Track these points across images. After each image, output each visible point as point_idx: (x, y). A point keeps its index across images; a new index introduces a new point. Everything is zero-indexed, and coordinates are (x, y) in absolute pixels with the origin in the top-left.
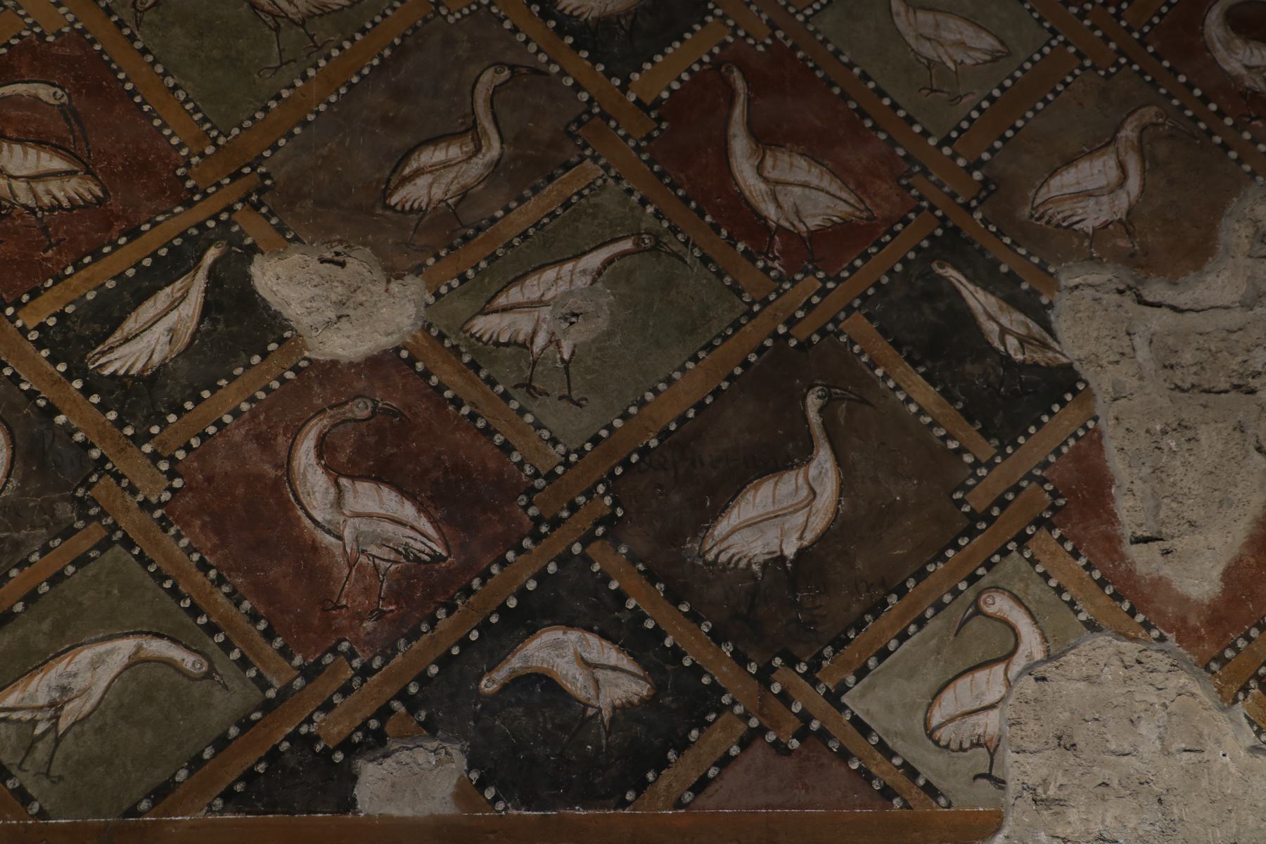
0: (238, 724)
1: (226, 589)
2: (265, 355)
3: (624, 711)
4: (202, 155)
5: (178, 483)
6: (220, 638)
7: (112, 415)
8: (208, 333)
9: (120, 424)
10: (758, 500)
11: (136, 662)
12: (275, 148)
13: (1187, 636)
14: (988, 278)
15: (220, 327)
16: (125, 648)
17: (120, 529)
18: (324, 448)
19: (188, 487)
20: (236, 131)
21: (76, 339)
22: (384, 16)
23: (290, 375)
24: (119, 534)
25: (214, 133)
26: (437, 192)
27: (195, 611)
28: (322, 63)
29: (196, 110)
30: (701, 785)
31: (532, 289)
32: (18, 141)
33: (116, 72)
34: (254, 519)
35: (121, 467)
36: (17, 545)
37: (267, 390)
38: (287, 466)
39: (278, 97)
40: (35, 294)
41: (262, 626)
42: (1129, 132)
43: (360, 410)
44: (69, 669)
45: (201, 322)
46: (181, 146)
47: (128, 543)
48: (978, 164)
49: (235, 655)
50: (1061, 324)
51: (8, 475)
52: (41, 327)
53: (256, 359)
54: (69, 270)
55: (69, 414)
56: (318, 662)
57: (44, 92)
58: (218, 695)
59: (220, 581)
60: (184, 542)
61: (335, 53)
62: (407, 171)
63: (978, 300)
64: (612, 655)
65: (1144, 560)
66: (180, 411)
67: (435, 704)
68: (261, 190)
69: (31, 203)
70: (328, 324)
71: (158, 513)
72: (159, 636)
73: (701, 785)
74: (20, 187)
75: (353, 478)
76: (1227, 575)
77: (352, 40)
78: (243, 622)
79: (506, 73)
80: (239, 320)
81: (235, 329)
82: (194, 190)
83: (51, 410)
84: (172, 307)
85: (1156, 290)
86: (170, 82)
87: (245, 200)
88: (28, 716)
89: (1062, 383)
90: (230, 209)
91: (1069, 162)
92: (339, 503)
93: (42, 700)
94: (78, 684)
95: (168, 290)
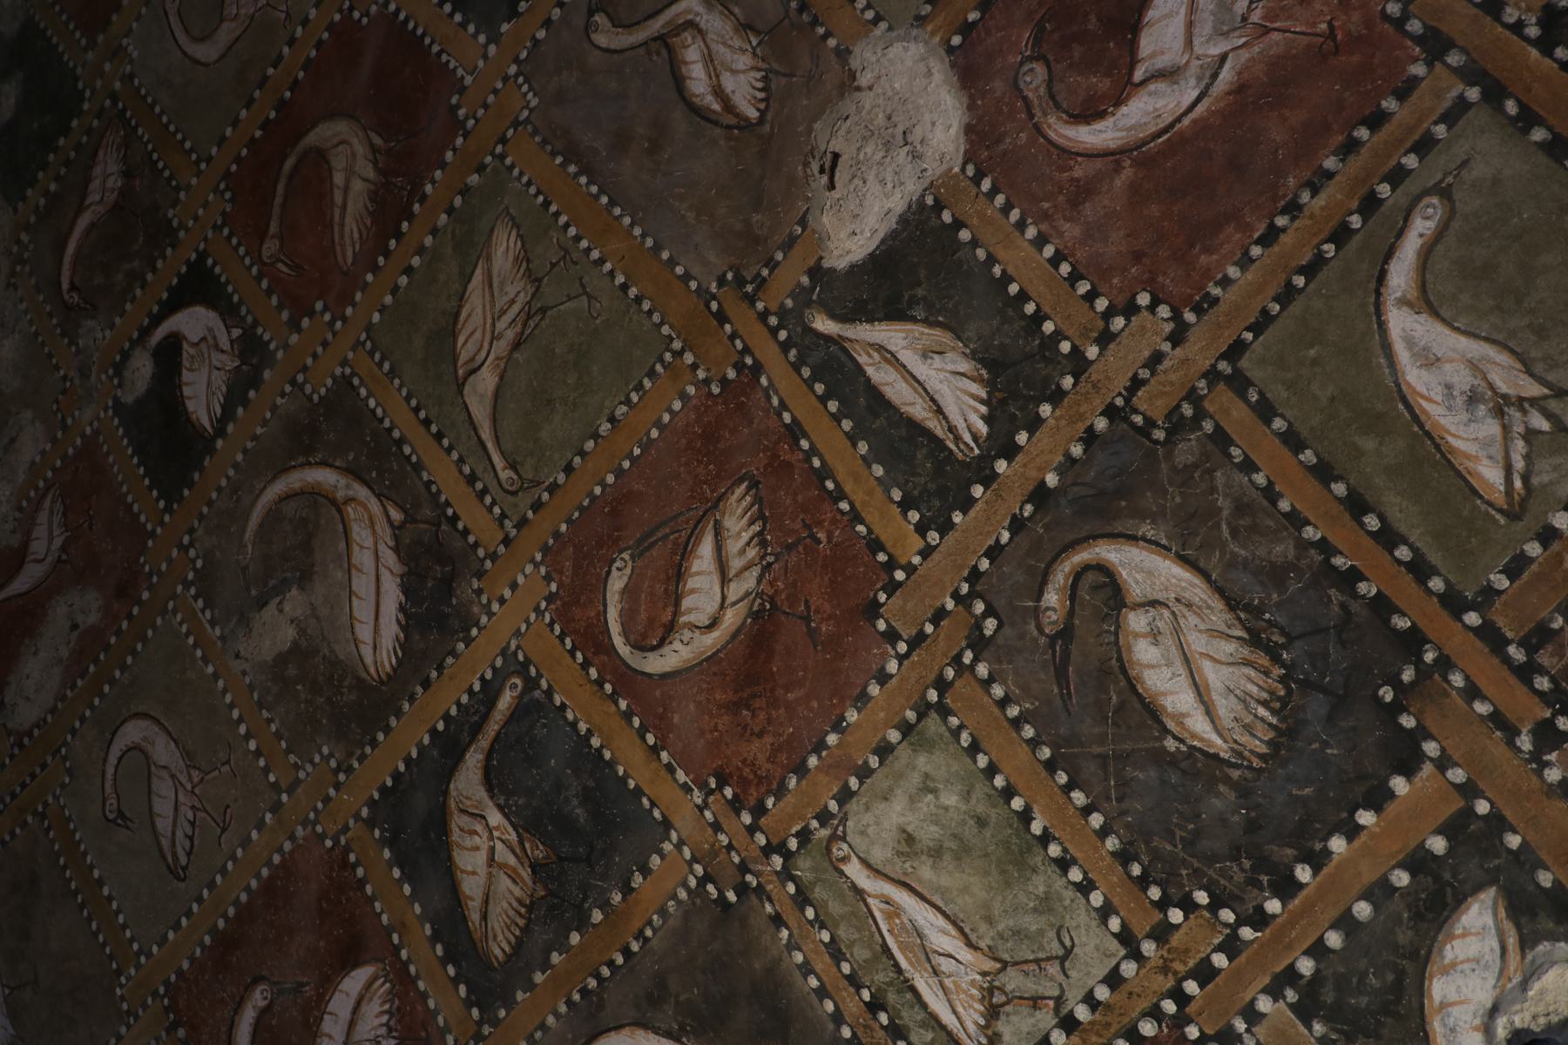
0: (1526, 130)
1: (1305, 197)
2: (958, 224)
4: (694, 367)
5: (1144, 299)
6: (1384, 190)
7: (1045, 410)
8: (930, 307)
9: (1057, 396)
11: (1426, 301)
12: (687, 277)
15: (920, 292)
16: (1399, 322)
17: (1214, 366)
18: (1089, 113)
19: (1150, 284)
20: (666, 330)
21: (935, 475)
22: (529, 183)
23: (986, 185)
24: (1224, 366)
25: (668, 356)
26: (744, 61)
27: (1341, 235)
28: (584, 244)
29: (639, 387)
32: (677, 604)
33: (594, 498)
34: (1196, 186)
35: (1122, 382)
36: (1241, 508)
37: (1006, 209)
38: (1113, 156)
39: (624, 287)
40: (876, 545)
41: (1363, 133)
43: (1035, 78)
44: (1439, 398)
45: (914, 320)
46: (683, 396)
47: (1236, 350)
49: (1411, 161)
51: (1133, 539)
52: (921, 529)
53: (965, 235)
54: (844, 506)
55: (1043, 470)
56: (1419, 40)
57: (616, 583)
58: (1479, 171)
59: (1293, 209)
60: (1233, 272)
61: (572, 231)
62: (716, 107)
66: (1039, 317)
68: (740, 282)
69: (755, 572)
70: (916, 156)
71: (1190, 317)
72: (1382, 277)
74: (735, 590)
75: (1133, 63)
77: (557, 214)
78: (1357, 162)
79: (599, 18)
81: (923, 273)
82: (739, 367)
83: (1040, 494)
84: (893, 360)
86: (605, 427)
87: (751, 300)
88: (1519, 446)
90: (763, 316)
92: (1170, 75)
93: (1492, 428)
94: (1463, 379)
95: (870, 371)
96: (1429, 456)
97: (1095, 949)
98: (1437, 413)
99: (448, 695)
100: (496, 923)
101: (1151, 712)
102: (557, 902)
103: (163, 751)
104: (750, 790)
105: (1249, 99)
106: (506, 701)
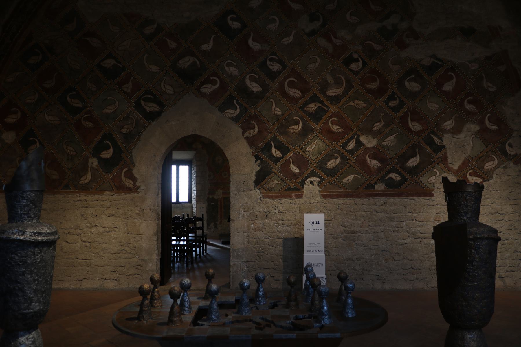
3: (399, 181)
10: (411, 160)
11: (355, 177)
13: (454, 173)
14: (436, 135)
16: (353, 175)
21: (344, 146)
30: (406, 187)
31: (388, 139)
34: (363, 163)
38: (366, 158)
42: (454, 117)
43: (372, 152)
48: (436, 122)
50: (444, 140)
57: (336, 119)
63: (435, 138)
64: (398, 175)
65: (450, 165)
67: (382, 180)
73: (406, 187)
76: (459, 167)
80: (359, 144)
85: (455, 136)
89: (444, 147)
91: (446, 121)
96: (345, 177)
97: (314, 158)
98: (347, 178)
99: (325, 102)
100: (308, 109)
101: (329, 161)
102: (310, 114)
103: (317, 64)
104: (321, 132)
105: (368, 167)
106: (326, 108)
